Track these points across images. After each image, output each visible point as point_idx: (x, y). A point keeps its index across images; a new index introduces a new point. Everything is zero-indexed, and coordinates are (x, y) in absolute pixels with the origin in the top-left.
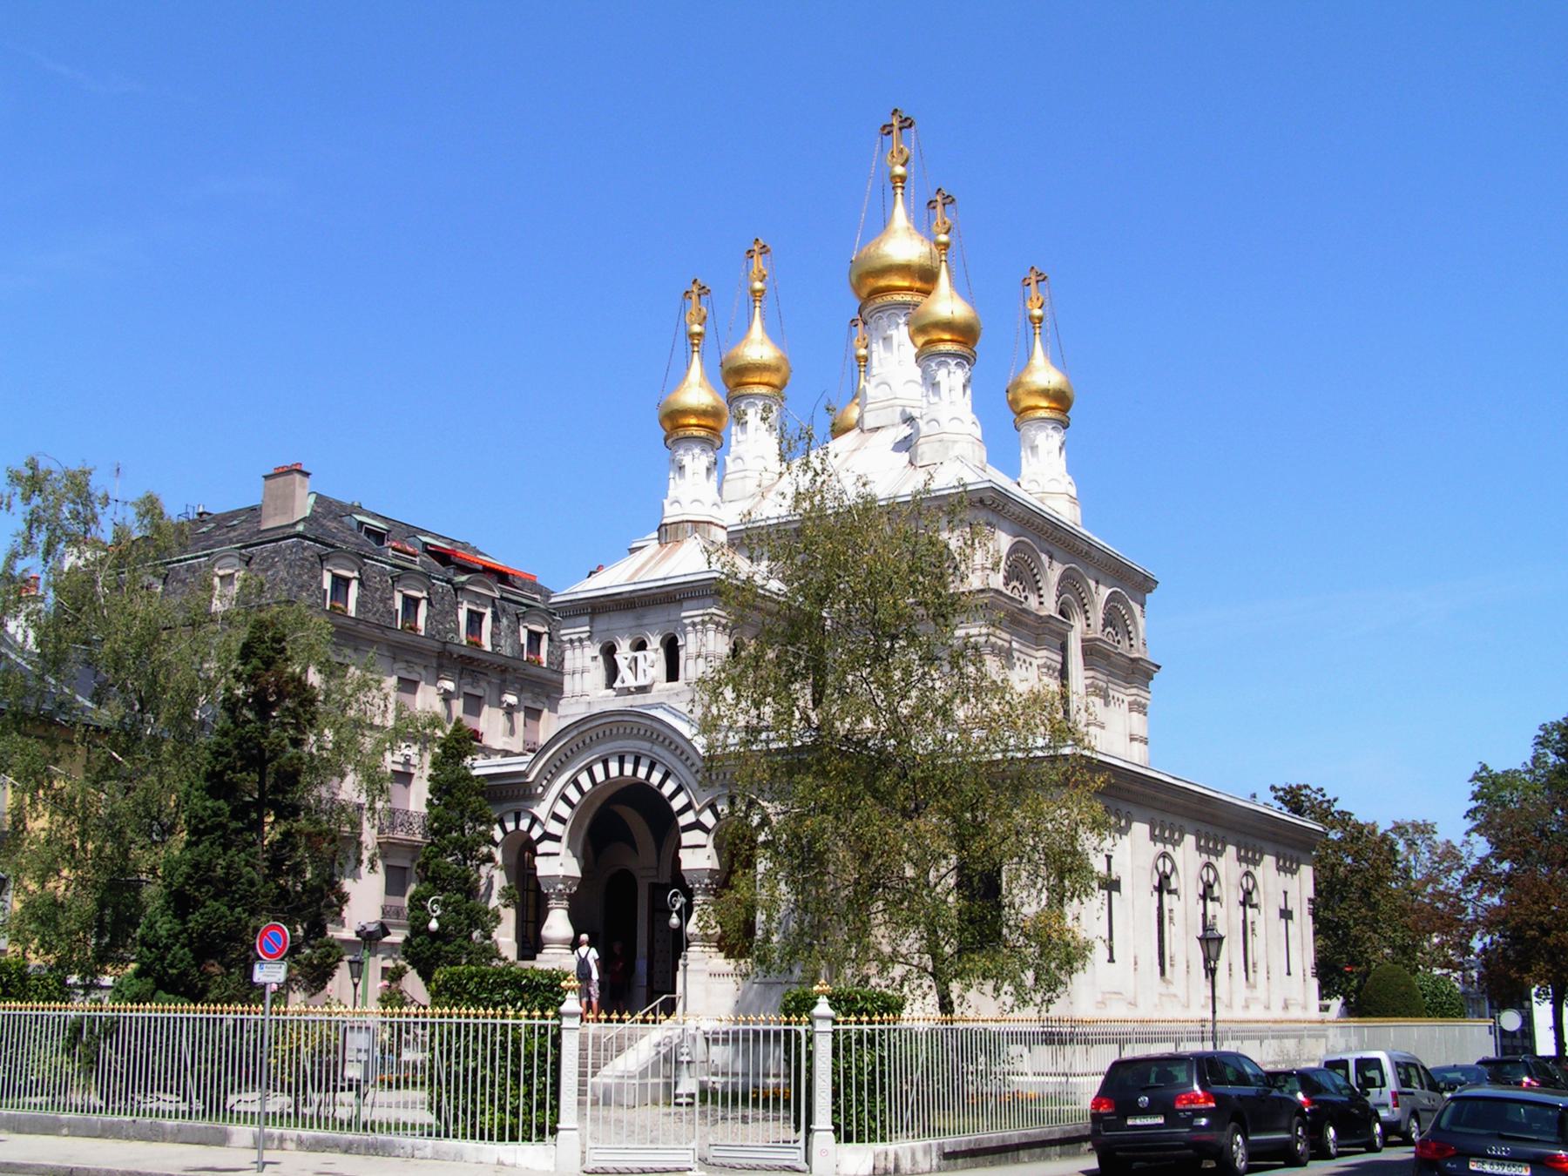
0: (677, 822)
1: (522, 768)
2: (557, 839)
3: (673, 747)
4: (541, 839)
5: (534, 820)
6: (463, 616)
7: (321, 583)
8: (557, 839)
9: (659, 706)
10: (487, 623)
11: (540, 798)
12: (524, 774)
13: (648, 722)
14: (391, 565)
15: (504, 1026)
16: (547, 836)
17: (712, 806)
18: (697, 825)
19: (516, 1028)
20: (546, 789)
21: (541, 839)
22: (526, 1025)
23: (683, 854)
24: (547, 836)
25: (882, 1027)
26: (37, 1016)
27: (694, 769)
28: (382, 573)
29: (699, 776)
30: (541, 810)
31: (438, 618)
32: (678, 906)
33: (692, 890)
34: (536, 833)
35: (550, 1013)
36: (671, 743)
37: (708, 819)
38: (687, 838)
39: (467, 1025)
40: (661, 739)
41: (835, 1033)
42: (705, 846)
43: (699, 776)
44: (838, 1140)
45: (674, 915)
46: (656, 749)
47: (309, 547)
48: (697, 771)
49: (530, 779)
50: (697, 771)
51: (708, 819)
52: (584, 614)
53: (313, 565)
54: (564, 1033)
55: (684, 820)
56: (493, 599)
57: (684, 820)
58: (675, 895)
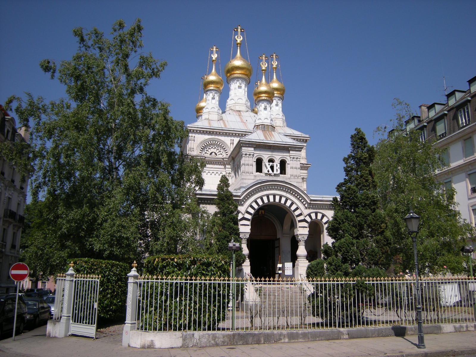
1: (239, 194)
2: (247, 220)
4: (242, 219)
8: (247, 220)
11: (242, 205)
12: (239, 196)
15: (167, 284)
16: (244, 219)
17: (309, 215)
18: (304, 220)
20: (244, 202)
21: (242, 219)
24: (244, 219)
26: (86, 281)
37: (309, 220)
38: (300, 224)
39: (392, 284)
42: (307, 227)
49: (241, 198)
51: (309, 220)
52: (252, 147)
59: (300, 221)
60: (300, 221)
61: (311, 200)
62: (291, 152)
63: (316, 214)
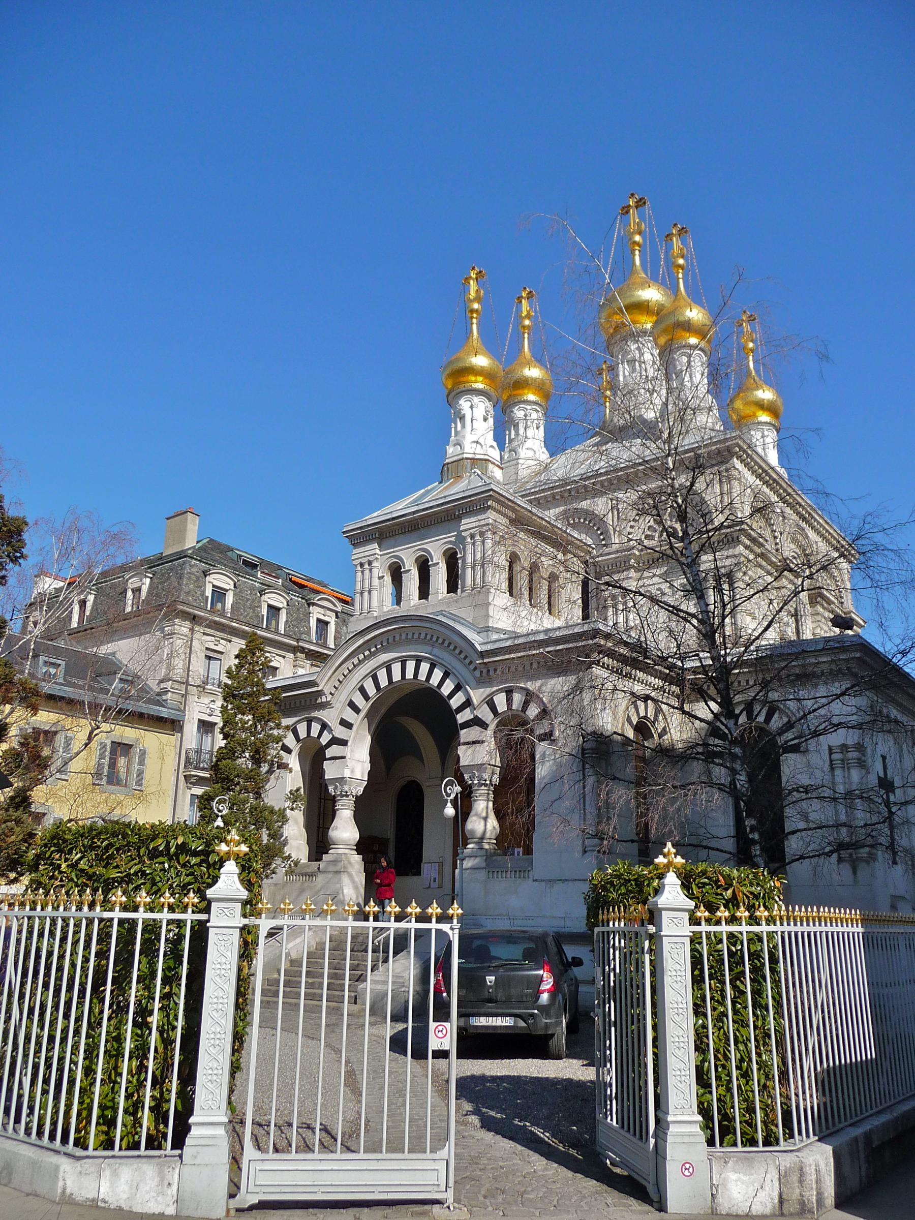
0: (456, 720)
3: (452, 647)
4: (329, 744)
5: (324, 726)
6: (313, 623)
7: (204, 591)
9: (441, 613)
10: (332, 629)
13: (428, 625)
14: (262, 584)
16: (335, 741)
18: (478, 722)
19: (152, 928)
21: (329, 744)
22: (121, 922)
23: (461, 750)
24: (335, 741)
25: (772, 928)
27: (472, 667)
28: (253, 588)
29: (477, 673)
30: (330, 716)
31: (294, 623)
32: (453, 796)
33: (471, 786)
34: (325, 739)
35: (192, 898)
36: (450, 644)
40: (440, 641)
41: (695, 940)
43: (477, 673)
44: (711, 1142)
45: (449, 804)
46: (436, 651)
47: (195, 565)
48: (475, 669)
50: (475, 669)
53: (198, 578)
54: (212, 933)
55: (461, 718)
56: (336, 613)
57: (461, 718)
58: (450, 783)
59: (467, 725)
60: (467, 725)
61: (483, 655)
62: (463, 522)
63: (509, 692)
